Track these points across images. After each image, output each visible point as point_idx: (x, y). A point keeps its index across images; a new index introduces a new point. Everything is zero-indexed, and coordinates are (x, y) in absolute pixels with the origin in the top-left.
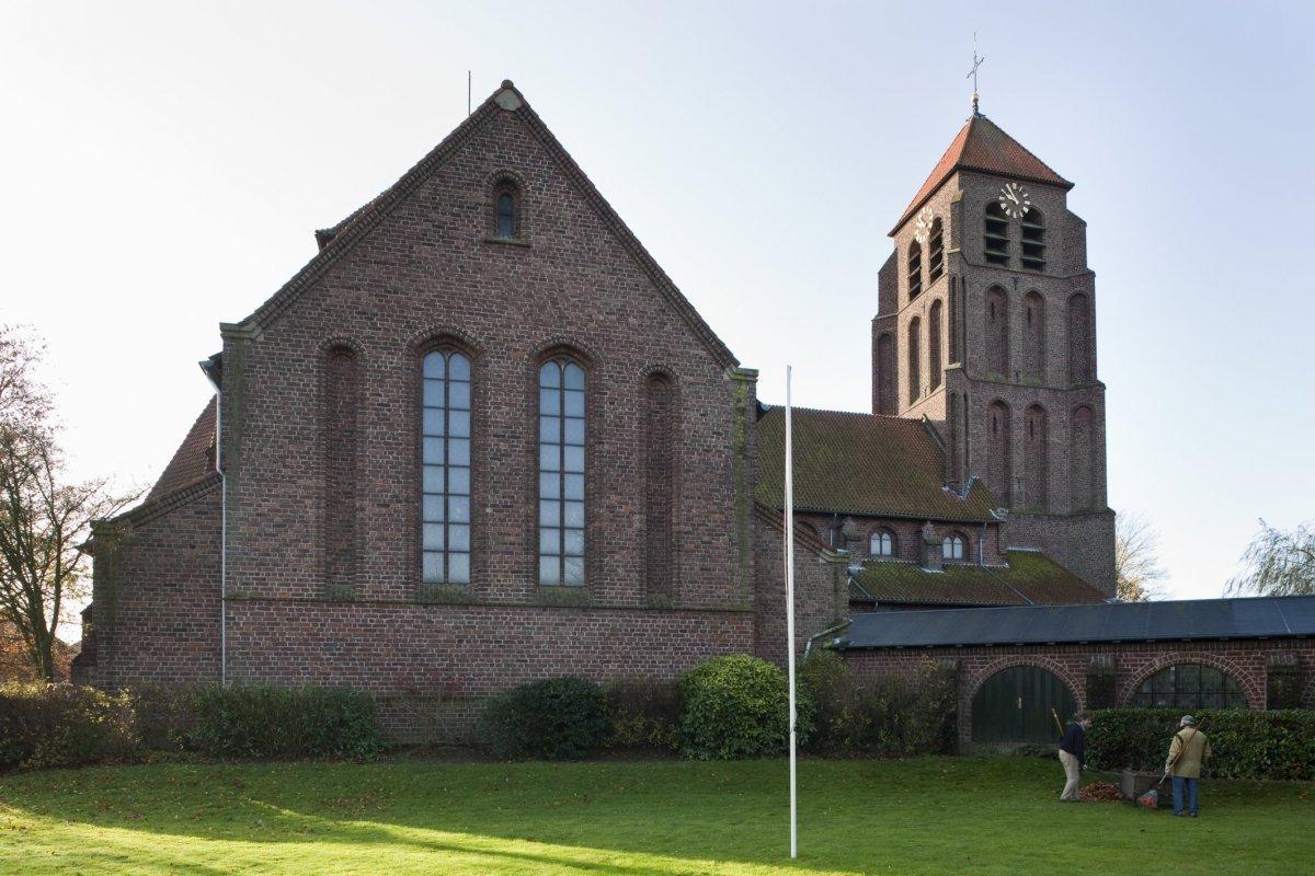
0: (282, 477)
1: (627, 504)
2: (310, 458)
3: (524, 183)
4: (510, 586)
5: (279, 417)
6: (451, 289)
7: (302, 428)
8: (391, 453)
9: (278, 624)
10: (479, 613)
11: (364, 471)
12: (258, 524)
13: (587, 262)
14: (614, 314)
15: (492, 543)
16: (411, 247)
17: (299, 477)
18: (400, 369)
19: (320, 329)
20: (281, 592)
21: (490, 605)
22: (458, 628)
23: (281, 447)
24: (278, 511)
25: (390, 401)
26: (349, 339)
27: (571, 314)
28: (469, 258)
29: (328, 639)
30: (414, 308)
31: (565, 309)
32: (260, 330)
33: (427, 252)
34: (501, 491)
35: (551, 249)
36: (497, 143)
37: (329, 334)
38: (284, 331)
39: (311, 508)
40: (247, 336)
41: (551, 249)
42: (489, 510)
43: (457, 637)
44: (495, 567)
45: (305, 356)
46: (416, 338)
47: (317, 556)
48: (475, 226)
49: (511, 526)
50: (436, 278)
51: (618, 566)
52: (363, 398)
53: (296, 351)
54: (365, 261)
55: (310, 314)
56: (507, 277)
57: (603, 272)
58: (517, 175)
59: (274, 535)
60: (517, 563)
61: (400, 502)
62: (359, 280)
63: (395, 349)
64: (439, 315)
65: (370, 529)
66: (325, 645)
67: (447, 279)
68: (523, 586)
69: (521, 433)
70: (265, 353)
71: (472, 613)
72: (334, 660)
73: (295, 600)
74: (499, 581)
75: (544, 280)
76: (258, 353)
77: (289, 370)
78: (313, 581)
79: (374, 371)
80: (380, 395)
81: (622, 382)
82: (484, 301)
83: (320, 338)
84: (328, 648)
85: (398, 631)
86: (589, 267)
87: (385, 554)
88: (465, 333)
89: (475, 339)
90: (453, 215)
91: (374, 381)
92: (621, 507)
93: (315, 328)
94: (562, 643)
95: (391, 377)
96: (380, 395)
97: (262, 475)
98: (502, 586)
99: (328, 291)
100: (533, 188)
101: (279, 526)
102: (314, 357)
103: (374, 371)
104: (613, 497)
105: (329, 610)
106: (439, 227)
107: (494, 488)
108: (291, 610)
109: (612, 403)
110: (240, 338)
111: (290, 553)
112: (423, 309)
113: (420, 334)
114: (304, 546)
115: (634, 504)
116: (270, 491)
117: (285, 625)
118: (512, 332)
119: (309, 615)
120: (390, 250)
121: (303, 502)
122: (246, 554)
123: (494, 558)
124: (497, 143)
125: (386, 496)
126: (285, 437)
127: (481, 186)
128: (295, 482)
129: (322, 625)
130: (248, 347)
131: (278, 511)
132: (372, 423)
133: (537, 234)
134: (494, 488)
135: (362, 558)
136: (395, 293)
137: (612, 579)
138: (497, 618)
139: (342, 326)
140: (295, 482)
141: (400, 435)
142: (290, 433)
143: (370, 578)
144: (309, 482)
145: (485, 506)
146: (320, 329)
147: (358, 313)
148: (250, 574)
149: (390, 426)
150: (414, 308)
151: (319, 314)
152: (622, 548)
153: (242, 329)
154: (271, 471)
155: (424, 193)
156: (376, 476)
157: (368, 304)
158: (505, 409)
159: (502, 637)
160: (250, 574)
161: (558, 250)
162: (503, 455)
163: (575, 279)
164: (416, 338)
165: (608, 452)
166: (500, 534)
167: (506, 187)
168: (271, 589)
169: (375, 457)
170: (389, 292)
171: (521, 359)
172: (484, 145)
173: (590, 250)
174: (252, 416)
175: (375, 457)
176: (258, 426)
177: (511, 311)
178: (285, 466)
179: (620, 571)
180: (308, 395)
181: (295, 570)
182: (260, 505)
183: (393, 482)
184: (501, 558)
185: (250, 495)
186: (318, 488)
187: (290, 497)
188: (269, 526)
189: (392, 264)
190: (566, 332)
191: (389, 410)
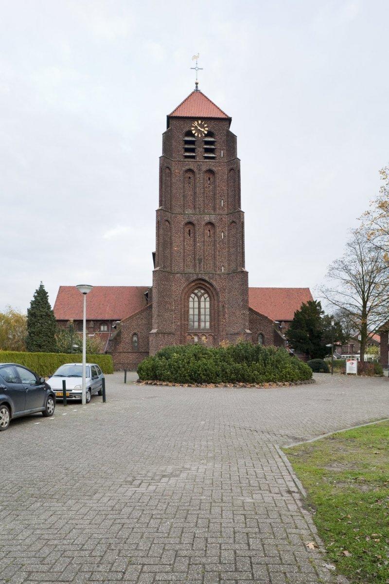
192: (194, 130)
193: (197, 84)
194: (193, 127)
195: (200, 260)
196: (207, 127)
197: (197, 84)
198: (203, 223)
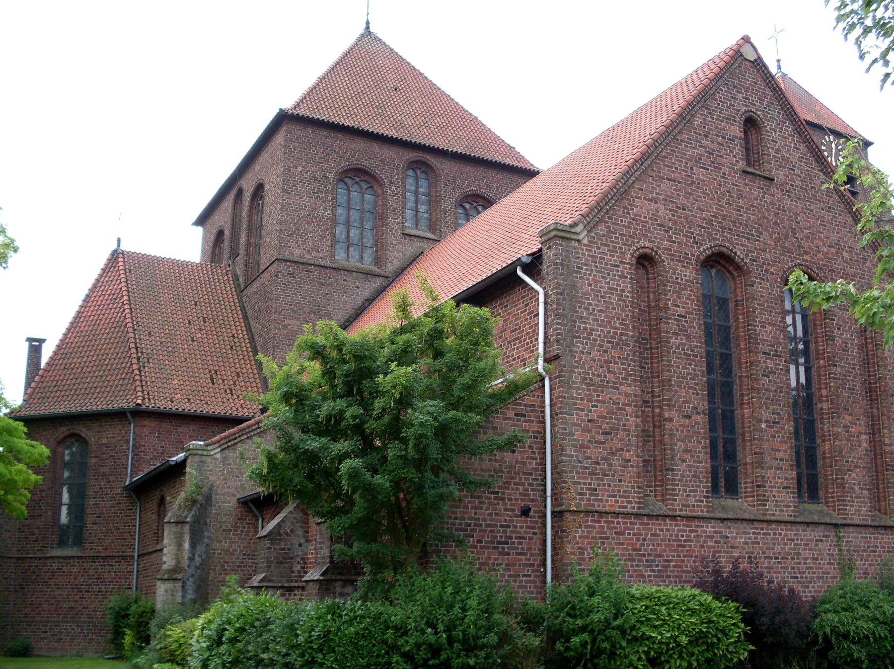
0: (608, 382)
1: (856, 424)
2: (629, 365)
3: (764, 123)
4: (782, 501)
5: (603, 321)
6: (723, 211)
7: (622, 334)
8: (690, 364)
9: (608, 538)
10: (762, 529)
11: (670, 381)
12: (590, 431)
13: (811, 198)
14: (833, 247)
15: (767, 459)
16: (692, 169)
17: (621, 384)
18: (692, 282)
19: (630, 236)
20: (609, 504)
21: (771, 521)
22: (747, 543)
23: (605, 351)
24: (605, 418)
25: (687, 313)
26: (652, 249)
27: (805, 244)
28: (733, 184)
29: (649, 555)
30: (699, 226)
31: (801, 239)
32: (585, 232)
33: (703, 175)
34: (771, 408)
35: (787, 184)
36: (743, 87)
37: (638, 243)
38: (603, 236)
39: (631, 416)
40: (575, 237)
41: (787, 184)
42: (763, 426)
43: (747, 553)
44: (771, 482)
45: (621, 262)
46: (701, 253)
47: (638, 467)
48: (735, 157)
49: (781, 442)
50: (712, 199)
51: (854, 484)
52: (666, 309)
53: (613, 256)
54: (660, 177)
55: (622, 221)
56: (760, 205)
57: (822, 209)
58: (759, 116)
59: (603, 443)
60: (786, 479)
61: (698, 413)
62: (658, 194)
63: (687, 263)
64: (716, 234)
65: (678, 440)
66: (647, 561)
67: (719, 201)
68: (791, 502)
69: (781, 352)
70: (589, 255)
71: (757, 529)
72: (655, 576)
73: (623, 514)
74: (774, 496)
75: (785, 211)
76: (583, 254)
77: (609, 274)
78: (635, 492)
79: (673, 282)
80: (679, 307)
81: (844, 309)
82: (746, 225)
83: (630, 245)
84: (650, 564)
85: (702, 546)
86: (812, 202)
87: (690, 466)
88: (735, 253)
89: (743, 260)
90: (719, 144)
91: (674, 292)
92: (852, 428)
93: (625, 236)
94: (822, 559)
95: (685, 289)
96: (679, 307)
97: (591, 379)
98: (776, 501)
99: (634, 201)
100: (770, 128)
101: (607, 434)
102: (628, 264)
103: (673, 282)
104: (846, 417)
105: (648, 524)
106: (710, 153)
107: (765, 403)
108: (618, 523)
109: (839, 329)
110: (567, 239)
111: (616, 461)
112: (703, 227)
113: (705, 250)
114: (627, 455)
115: (860, 425)
116: (598, 396)
117: (613, 538)
118: (768, 256)
119: (633, 529)
120: (676, 168)
121: (624, 410)
122: (579, 461)
123: (770, 473)
124: (743, 87)
125: (689, 407)
126: (609, 342)
127: (735, 121)
128: (617, 389)
129: (644, 540)
130: (575, 248)
131: (605, 418)
132: (674, 333)
133: (777, 169)
134: (765, 403)
135: (672, 470)
136: (683, 210)
137: (851, 497)
138: (775, 534)
139: (647, 236)
140: (617, 389)
141: (696, 347)
142: (612, 337)
143: (679, 490)
144: (629, 390)
145: (760, 421)
146: (630, 236)
147: (658, 225)
148: (585, 484)
149: (688, 337)
150: (699, 226)
151: (629, 223)
152: (856, 467)
153: (573, 230)
154: (599, 376)
155: (697, 121)
156: (679, 386)
157: (664, 218)
158: (769, 328)
159: (779, 553)
160: (585, 484)
161: (792, 185)
162: (771, 372)
163: (805, 213)
164: (701, 253)
165: (840, 374)
166: (773, 449)
167: (751, 123)
168: (601, 500)
169: (678, 367)
170: (679, 208)
171: (776, 281)
172: (735, 87)
173: (812, 188)
174: (581, 318)
175: (678, 367)
176: (585, 329)
177: (765, 236)
178: (609, 372)
179: (857, 488)
180: (624, 301)
181: (620, 481)
182: (590, 411)
183: (693, 394)
184: (775, 473)
185: (582, 399)
186: (636, 396)
187: (614, 403)
188: (598, 433)
189: (680, 182)
190: (804, 260)
191: (686, 321)
193: (778, 61)
197: (778, 61)
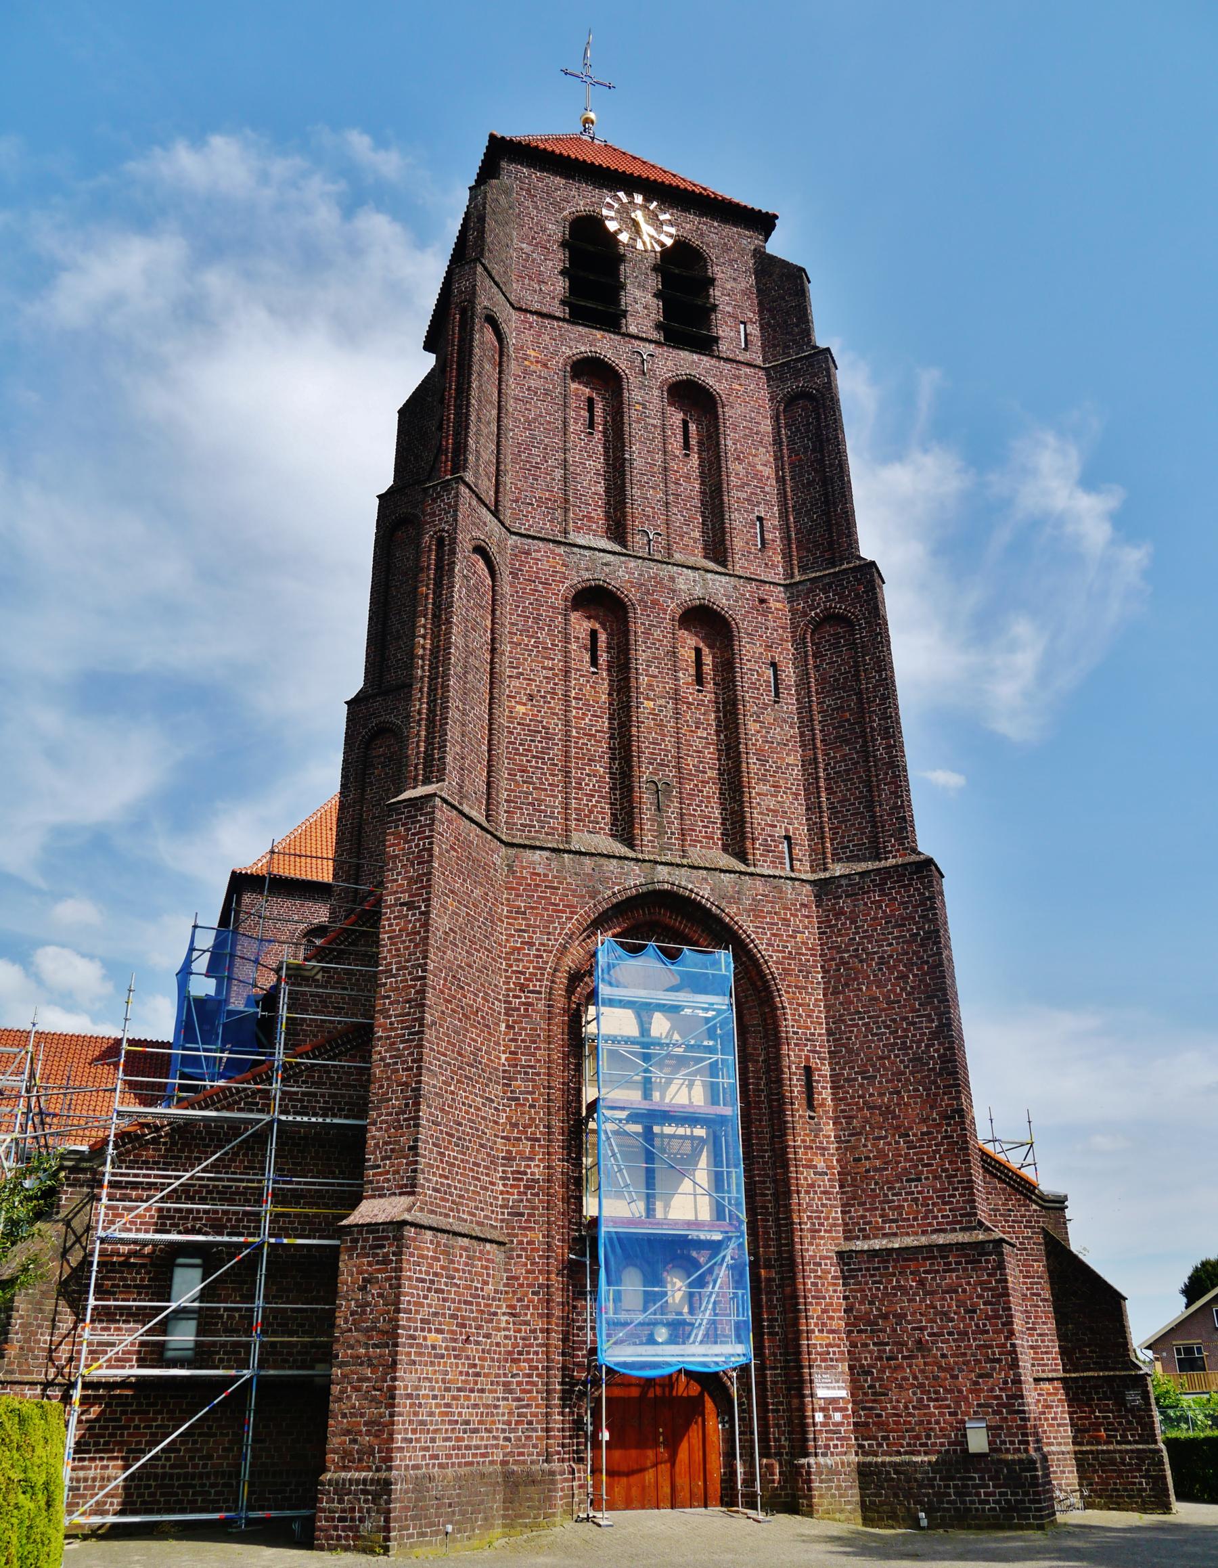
192: (612, 219)
194: (610, 206)
195: (660, 791)
196: (671, 224)
198: (673, 607)
